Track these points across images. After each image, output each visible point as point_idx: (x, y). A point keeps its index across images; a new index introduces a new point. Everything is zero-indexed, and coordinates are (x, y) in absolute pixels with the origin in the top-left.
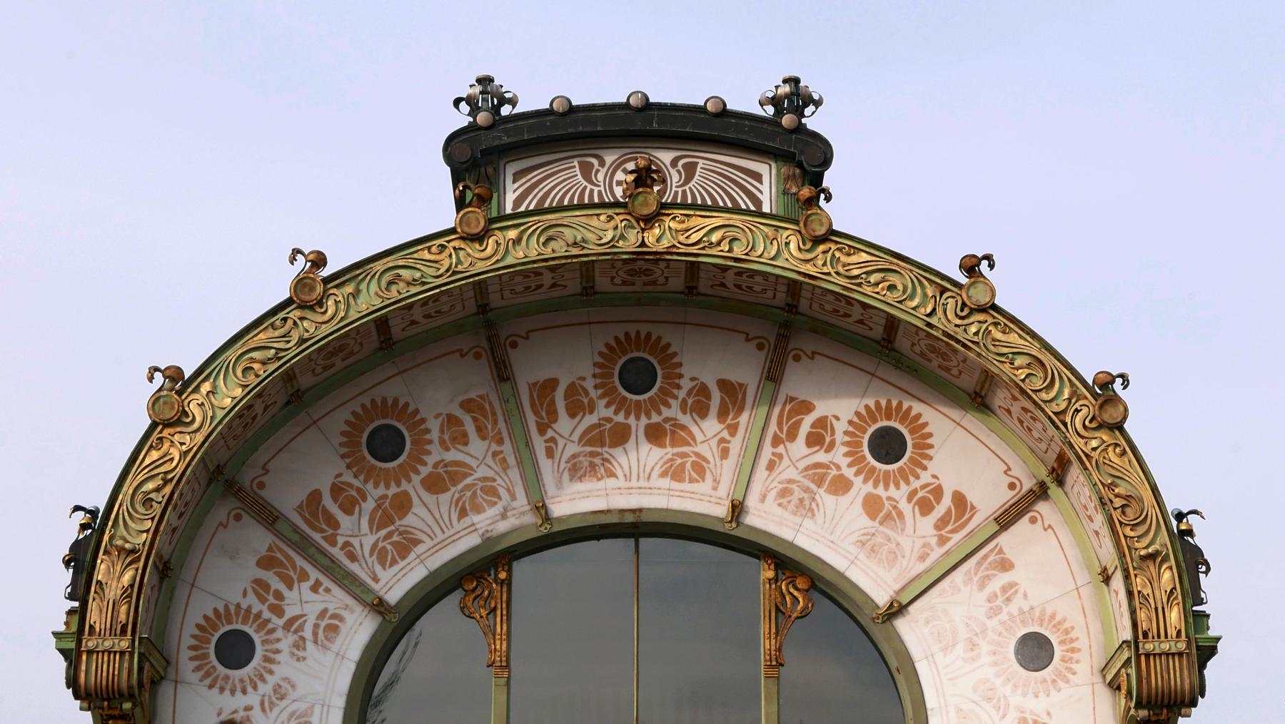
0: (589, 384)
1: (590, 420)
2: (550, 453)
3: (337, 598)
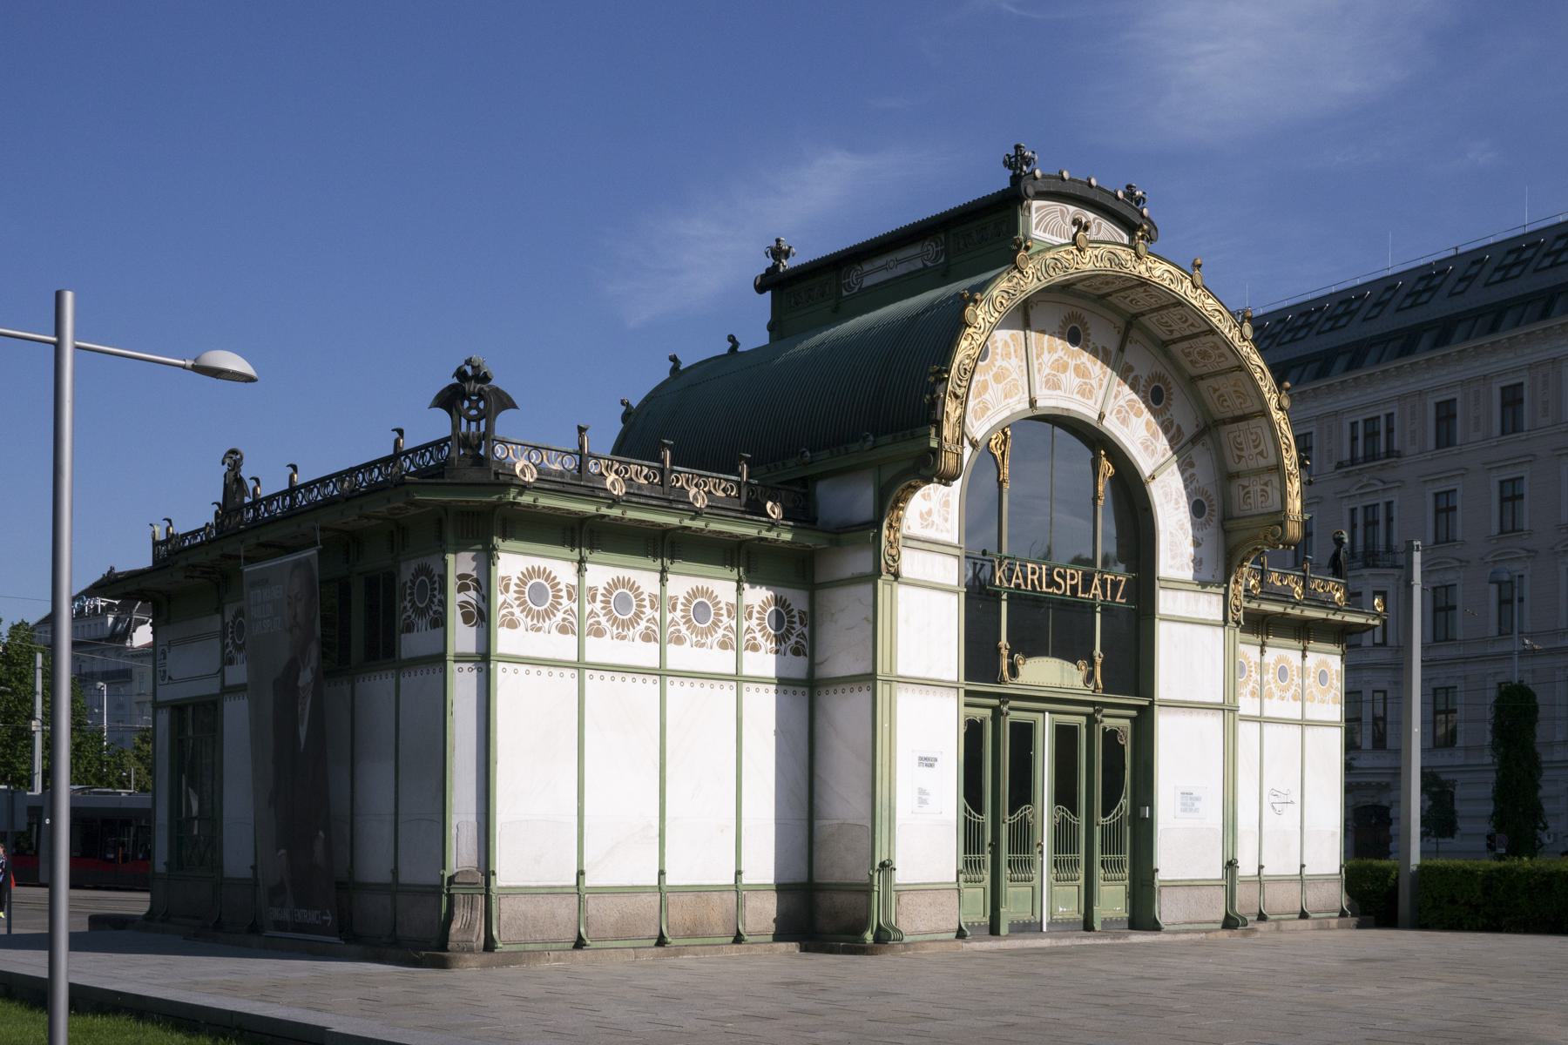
1: (1055, 356)
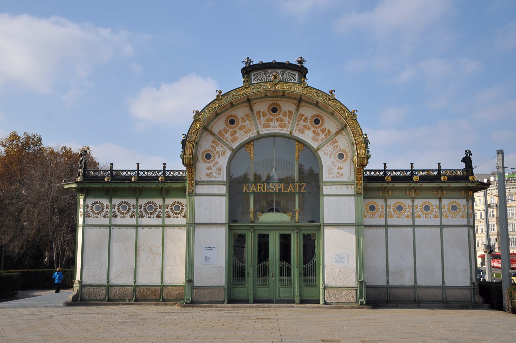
0: (266, 111)
1: (266, 118)
2: (260, 123)
3: (225, 148)
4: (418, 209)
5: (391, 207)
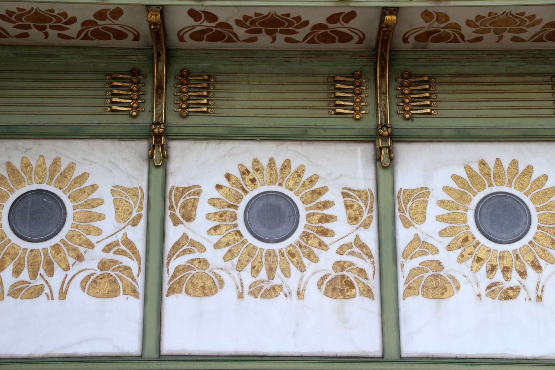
4: (431, 228)
5: (204, 208)
